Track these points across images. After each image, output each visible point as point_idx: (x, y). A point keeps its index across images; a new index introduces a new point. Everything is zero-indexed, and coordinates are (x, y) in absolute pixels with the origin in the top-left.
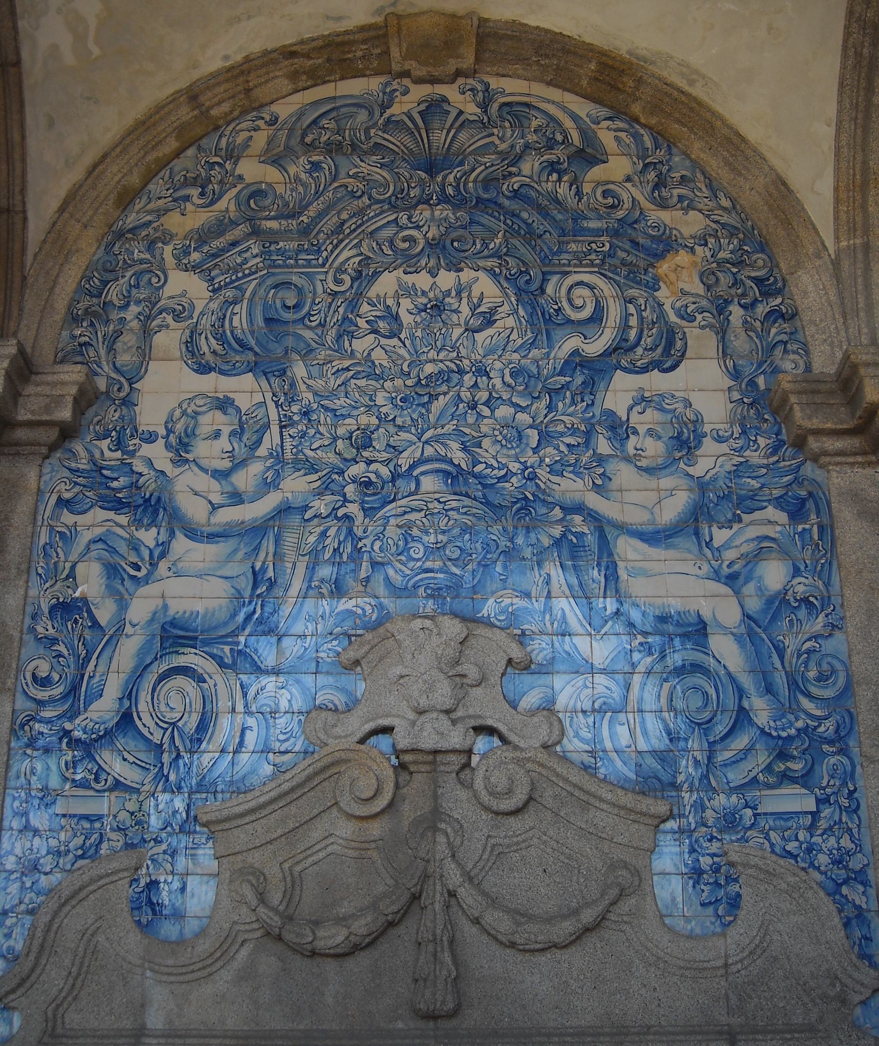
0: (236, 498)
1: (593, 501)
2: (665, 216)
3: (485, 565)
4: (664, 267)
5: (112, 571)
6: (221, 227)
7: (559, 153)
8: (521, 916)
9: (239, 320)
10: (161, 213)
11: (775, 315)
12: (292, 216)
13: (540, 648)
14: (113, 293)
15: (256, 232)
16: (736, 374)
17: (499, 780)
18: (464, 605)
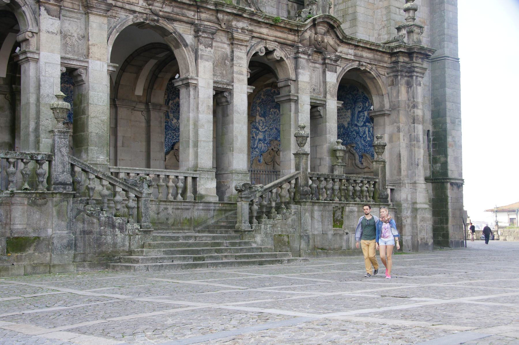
0: (263, 129)
5: (256, 134)
14: (254, 108)
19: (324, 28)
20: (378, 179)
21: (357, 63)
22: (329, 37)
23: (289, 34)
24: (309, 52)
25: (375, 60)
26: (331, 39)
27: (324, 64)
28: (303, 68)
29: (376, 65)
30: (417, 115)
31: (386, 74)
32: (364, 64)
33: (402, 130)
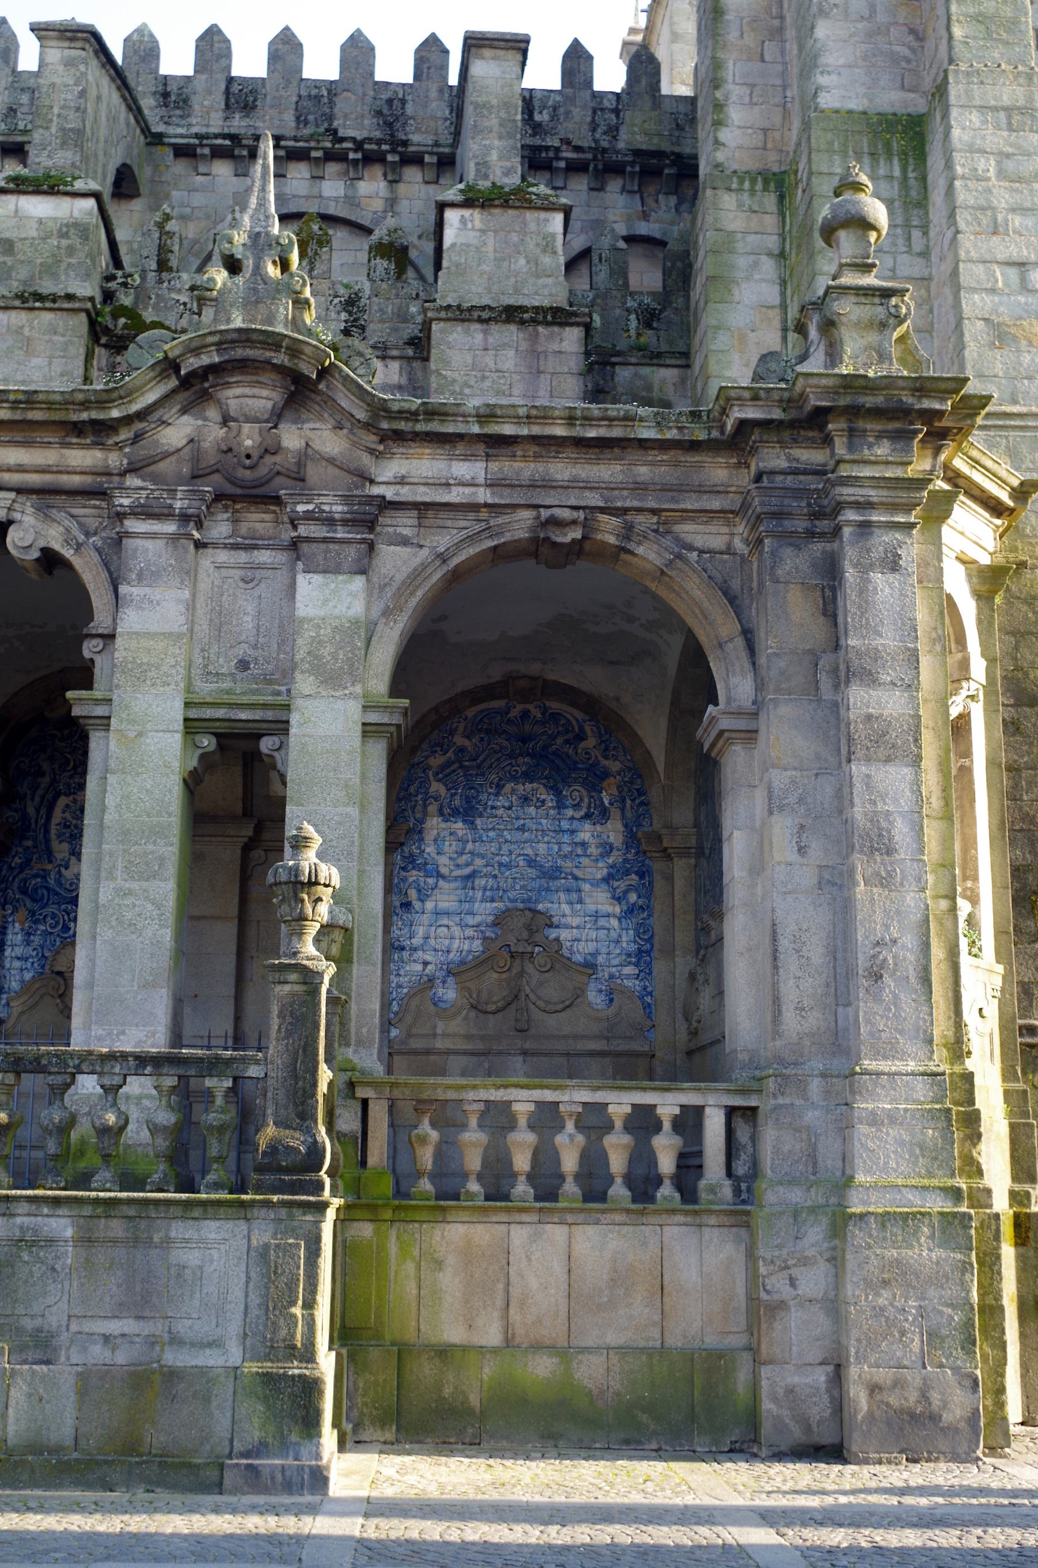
1: (576, 871)
2: (605, 762)
3: (539, 892)
4: (605, 784)
5: (419, 891)
6: (449, 764)
7: (570, 735)
8: (548, 1003)
9: (457, 802)
10: (427, 757)
11: (642, 804)
12: (475, 760)
13: (555, 920)
14: (412, 789)
15: (461, 767)
16: (626, 826)
17: (542, 962)
18: (532, 906)
19: (265, 393)
20: (257, 1062)
21: (527, 514)
22: (317, 425)
23: (68, 445)
24: (178, 504)
25: (640, 488)
26: (328, 435)
27: (294, 545)
28: (148, 576)
29: (654, 512)
30: (869, 717)
31: (738, 545)
32: (566, 514)
33: (792, 799)
